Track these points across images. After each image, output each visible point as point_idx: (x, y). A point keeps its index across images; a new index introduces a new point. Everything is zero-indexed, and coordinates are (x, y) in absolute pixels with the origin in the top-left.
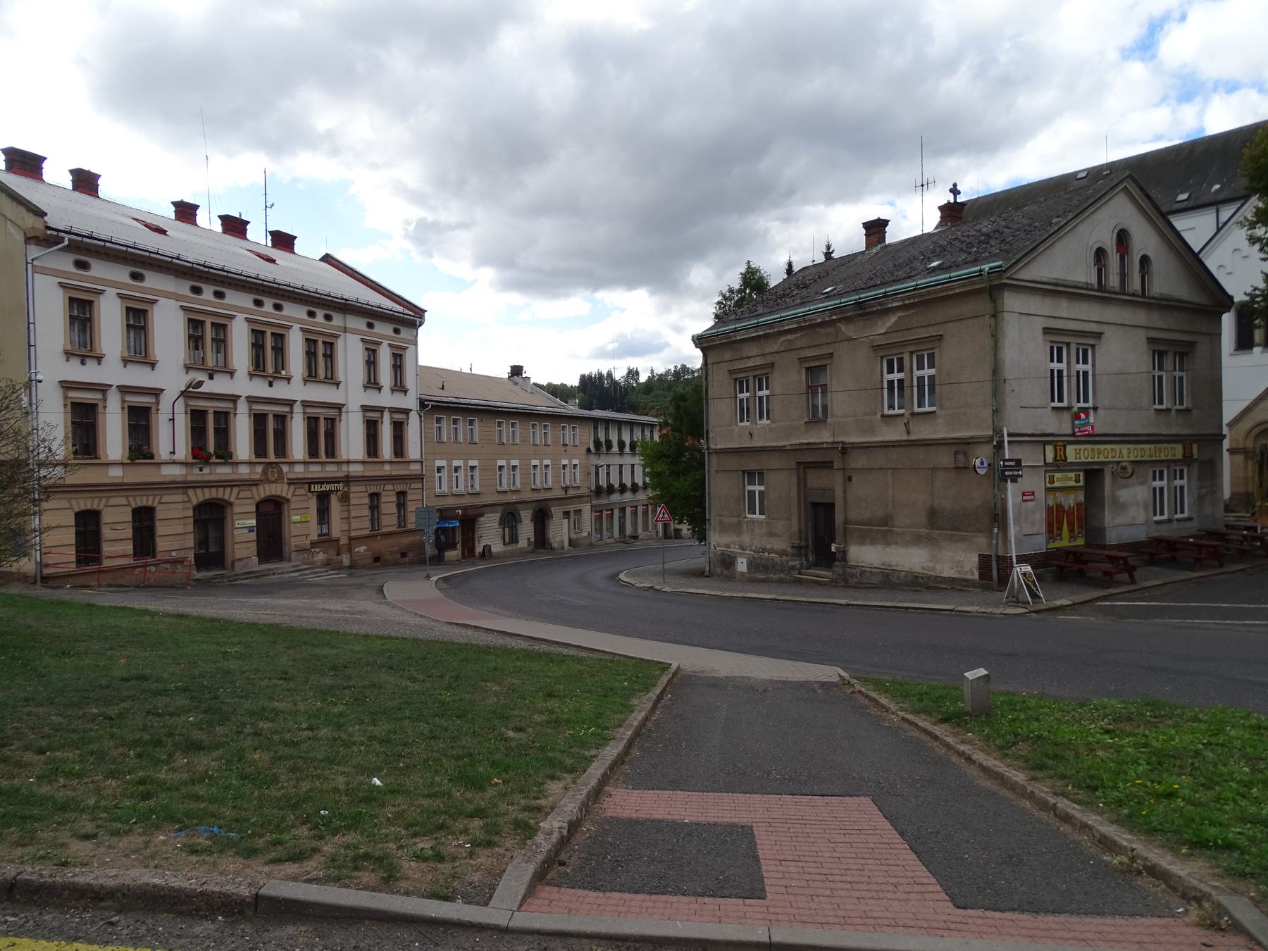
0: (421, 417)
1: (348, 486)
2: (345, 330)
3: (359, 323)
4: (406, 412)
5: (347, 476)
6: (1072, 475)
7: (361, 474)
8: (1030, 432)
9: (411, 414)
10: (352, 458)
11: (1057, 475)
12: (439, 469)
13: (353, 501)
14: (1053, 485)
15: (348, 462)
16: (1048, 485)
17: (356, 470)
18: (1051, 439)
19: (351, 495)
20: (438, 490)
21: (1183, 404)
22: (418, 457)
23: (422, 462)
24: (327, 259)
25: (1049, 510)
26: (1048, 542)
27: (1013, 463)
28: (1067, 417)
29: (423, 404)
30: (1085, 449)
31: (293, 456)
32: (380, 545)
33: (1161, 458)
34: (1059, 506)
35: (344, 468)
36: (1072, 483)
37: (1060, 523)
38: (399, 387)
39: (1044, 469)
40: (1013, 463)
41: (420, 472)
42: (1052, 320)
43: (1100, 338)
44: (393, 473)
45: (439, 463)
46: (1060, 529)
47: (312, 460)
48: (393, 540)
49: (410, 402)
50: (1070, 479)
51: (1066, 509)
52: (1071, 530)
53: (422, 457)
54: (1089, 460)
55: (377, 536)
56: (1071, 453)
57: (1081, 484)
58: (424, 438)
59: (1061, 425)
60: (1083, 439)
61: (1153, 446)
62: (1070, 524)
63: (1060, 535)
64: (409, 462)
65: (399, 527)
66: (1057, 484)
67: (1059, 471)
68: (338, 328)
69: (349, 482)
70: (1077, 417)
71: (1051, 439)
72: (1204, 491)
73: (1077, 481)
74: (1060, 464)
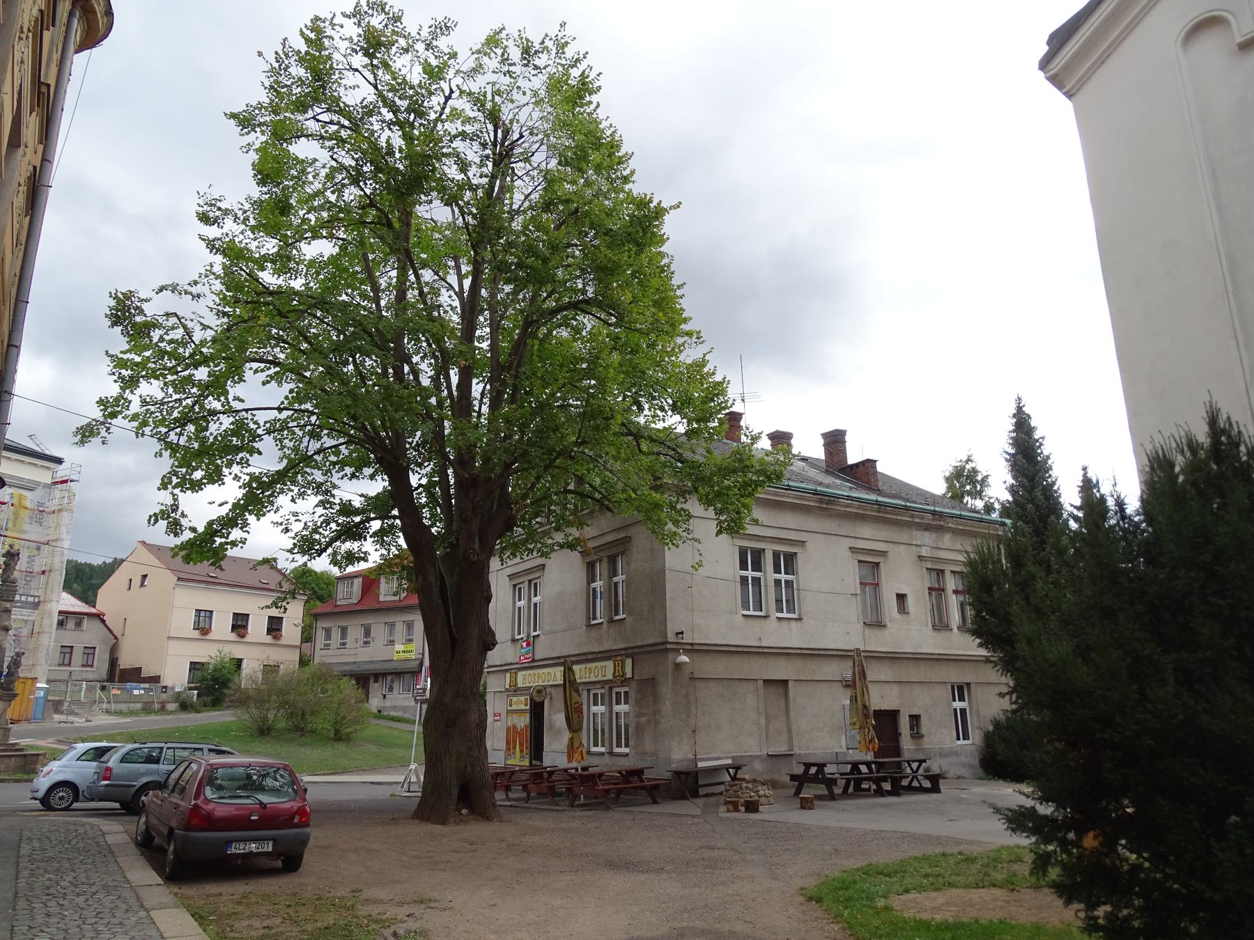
6: (523, 699)
8: (499, 664)
11: (514, 699)
14: (512, 708)
16: (509, 708)
18: (507, 667)
25: (508, 729)
26: (506, 759)
27: (421, 691)
30: (596, 667)
33: (591, 680)
34: (515, 727)
36: (523, 707)
37: (515, 742)
39: (506, 693)
40: (421, 691)
43: (544, 569)
46: (514, 748)
51: (519, 730)
52: (522, 751)
57: (528, 707)
60: (526, 665)
61: (583, 666)
62: (521, 745)
63: (514, 753)
66: (514, 707)
71: (507, 667)
72: (643, 719)
73: (526, 705)
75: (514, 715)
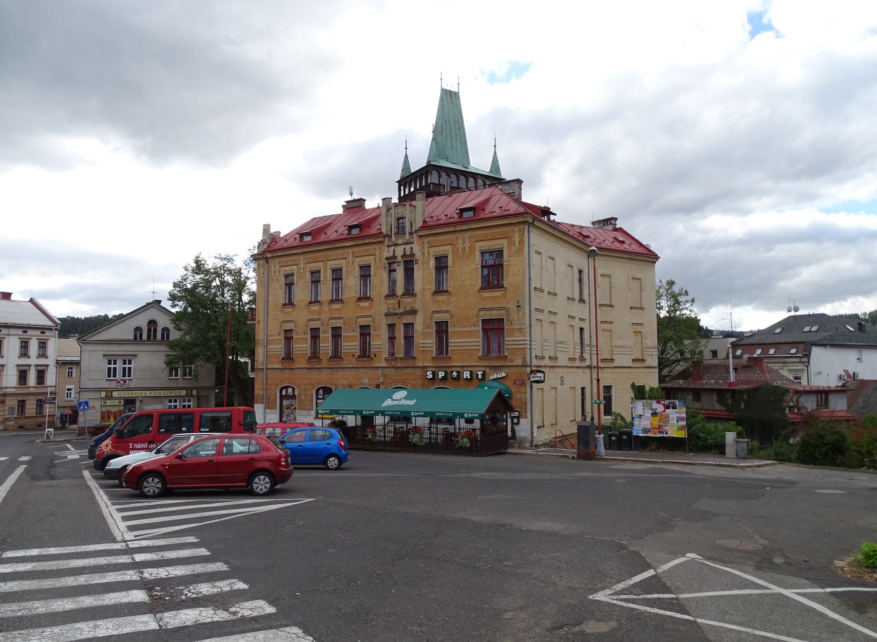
0: (57, 367)
1: (5, 397)
2: (9, 335)
3: (20, 332)
4: (47, 366)
5: (4, 394)
7: (14, 392)
9: (49, 368)
10: (8, 386)
11: (108, 401)
12: (68, 390)
13: (7, 404)
15: (6, 388)
16: (102, 404)
17: (8, 390)
18: (104, 389)
19: (7, 401)
20: (66, 399)
21: (177, 376)
22: (54, 384)
23: (56, 387)
24: (32, 301)
28: (115, 382)
29: (57, 362)
31: (30, 383)
32: (22, 422)
34: (109, 412)
35: (4, 390)
38: (43, 355)
41: (55, 391)
42: (109, 352)
44: (35, 392)
45: (68, 387)
47: (20, 386)
48: (32, 420)
49: (51, 361)
50: (116, 402)
53: (56, 384)
54: (126, 396)
55: (22, 417)
56: (115, 394)
57: (122, 403)
58: (58, 376)
59: (114, 385)
64: (46, 387)
65: (37, 413)
66: (107, 404)
67: (109, 399)
68: (4, 334)
69: (6, 395)
70: (119, 382)
74: (111, 397)
75: (108, 407)
